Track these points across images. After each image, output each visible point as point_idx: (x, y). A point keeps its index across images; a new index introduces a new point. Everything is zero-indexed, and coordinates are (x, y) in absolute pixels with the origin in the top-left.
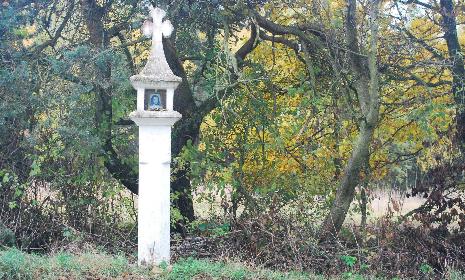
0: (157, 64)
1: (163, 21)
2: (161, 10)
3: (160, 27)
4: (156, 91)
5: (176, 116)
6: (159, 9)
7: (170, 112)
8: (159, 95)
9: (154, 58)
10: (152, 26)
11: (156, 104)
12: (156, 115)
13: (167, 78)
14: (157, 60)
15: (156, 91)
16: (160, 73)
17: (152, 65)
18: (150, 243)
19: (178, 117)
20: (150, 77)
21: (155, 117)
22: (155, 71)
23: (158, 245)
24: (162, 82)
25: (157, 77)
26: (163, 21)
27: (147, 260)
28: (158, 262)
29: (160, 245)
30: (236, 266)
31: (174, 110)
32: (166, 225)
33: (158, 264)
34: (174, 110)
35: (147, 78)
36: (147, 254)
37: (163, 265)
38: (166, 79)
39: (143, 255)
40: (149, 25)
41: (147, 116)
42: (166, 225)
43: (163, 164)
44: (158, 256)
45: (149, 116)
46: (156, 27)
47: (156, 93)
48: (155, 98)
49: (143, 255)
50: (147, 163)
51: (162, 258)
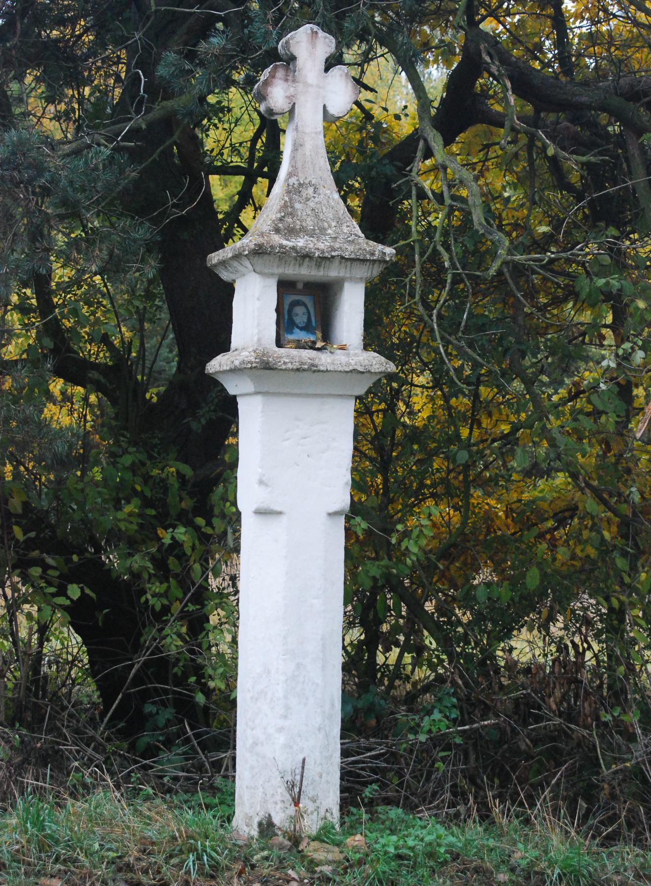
0: (311, 204)
1: (327, 70)
2: (321, 34)
3: (318, 86)
4: (300, 286)
5: (376, 368)
6: (315, 28)
7: (356, 355)
8: (308, 300)
9: (300, 184)
10: (294, 81)
11: (301, 329)
12: (316, 362)
13: (351, 248)
14: (311, 190)
15: (300, 286)
16: (323, 231)
17: (298, 206)
18: (289, 763)
19: (383, 369)
20: (300, 242)
21: (313, 369)
22: (310, 224)
23: (312, 770)
24: (336, 262)
25: (321, 246)
26: (327, 70)
27: (278, 819)
28: (311, 825)
29: (319, 769)
30: (555, 841)
31: (366, 347)
32: (333, 705)
33: (314, 832)
34: (366, 347)
35: (293, 248)
36: (278, 798)
37: (324, 835)
38: (349, 251)
39: (265, 801)
40: (286, 80)
41: (290, 366)
42: (333, 705)
43: (330, 514)
44: (311, 807)
45: (296, 365)
46: (306, 85)
47: (300, 292)
48: (299, 310)
49: (265, 801)
50: (280, 513)
51: (322, 814)
